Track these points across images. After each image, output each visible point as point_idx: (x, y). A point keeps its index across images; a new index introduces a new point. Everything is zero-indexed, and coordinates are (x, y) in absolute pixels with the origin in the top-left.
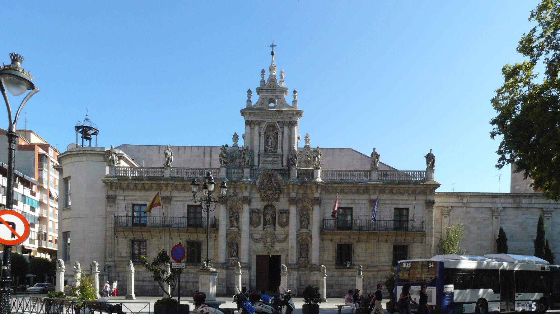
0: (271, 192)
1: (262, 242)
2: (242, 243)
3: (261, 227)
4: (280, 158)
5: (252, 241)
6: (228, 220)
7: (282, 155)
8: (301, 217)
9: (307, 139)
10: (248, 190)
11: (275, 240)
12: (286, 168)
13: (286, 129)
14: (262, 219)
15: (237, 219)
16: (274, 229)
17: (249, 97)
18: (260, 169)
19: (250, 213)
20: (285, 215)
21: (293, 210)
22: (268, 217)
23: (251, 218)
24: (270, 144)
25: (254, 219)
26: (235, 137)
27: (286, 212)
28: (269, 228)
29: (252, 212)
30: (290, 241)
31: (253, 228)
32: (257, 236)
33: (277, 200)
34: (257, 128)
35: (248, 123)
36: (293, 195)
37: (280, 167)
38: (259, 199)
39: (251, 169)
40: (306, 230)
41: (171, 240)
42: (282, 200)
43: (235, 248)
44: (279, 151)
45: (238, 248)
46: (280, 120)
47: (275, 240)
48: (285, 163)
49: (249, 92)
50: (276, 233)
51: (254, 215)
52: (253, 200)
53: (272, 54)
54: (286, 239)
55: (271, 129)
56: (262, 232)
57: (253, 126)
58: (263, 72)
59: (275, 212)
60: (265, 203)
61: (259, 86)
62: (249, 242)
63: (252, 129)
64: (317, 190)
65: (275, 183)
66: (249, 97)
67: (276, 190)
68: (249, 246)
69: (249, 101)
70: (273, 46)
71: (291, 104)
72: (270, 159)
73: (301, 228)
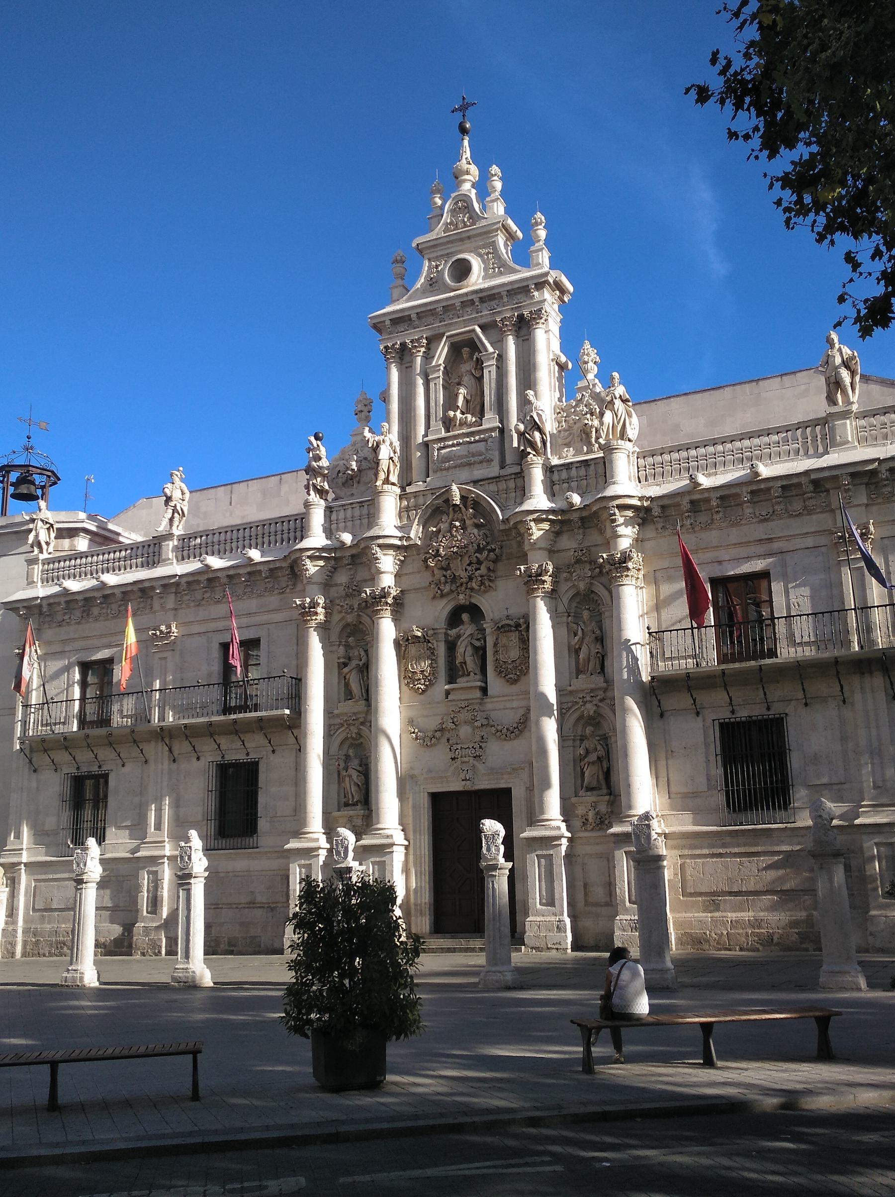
1: (444, 740)
12: (517, 469)
16: (484, 690)
20: (514, 637)
41: (174, 766)
43: (355, 775)
67: (479, 550)
73: (579, 672)
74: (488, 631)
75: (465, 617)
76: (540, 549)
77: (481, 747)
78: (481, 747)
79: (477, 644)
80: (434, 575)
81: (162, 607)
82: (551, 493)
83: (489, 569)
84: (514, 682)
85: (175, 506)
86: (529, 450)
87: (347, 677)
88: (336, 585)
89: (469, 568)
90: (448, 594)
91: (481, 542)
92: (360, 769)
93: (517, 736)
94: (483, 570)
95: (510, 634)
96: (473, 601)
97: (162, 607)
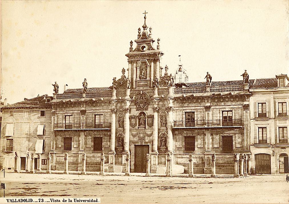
7: (150, 80)
13: (152, 64)
16: (145, 128)
17: (131, 46)
19: (129, 118)
21: (156, 115)
26: (124, 71)
27: (152, 117)
28: (142, 127)
29: (131, 118)
33: (146, 109)
34: (135, 64)
35: (130, 62)
38: (135, 110)
44: (148, 78)
49: (131, 43)
51: (133, 120)
53: (145, 18)
54: (152, 134)
57: (133, 63)
58: (139, 29)
63: (132, 65)
66: (131, 46)
69: (131, 49)
70: (145, 13)
71: (156, 48)
74: (146, 117)
79: (144, 119)
80: (137, 106)
81: (83, 107)
82: (159, 94)
85: (85, 87)
86: (155, 86)
94: (146, 107)
96: (144, 112)
97: (83, 107)
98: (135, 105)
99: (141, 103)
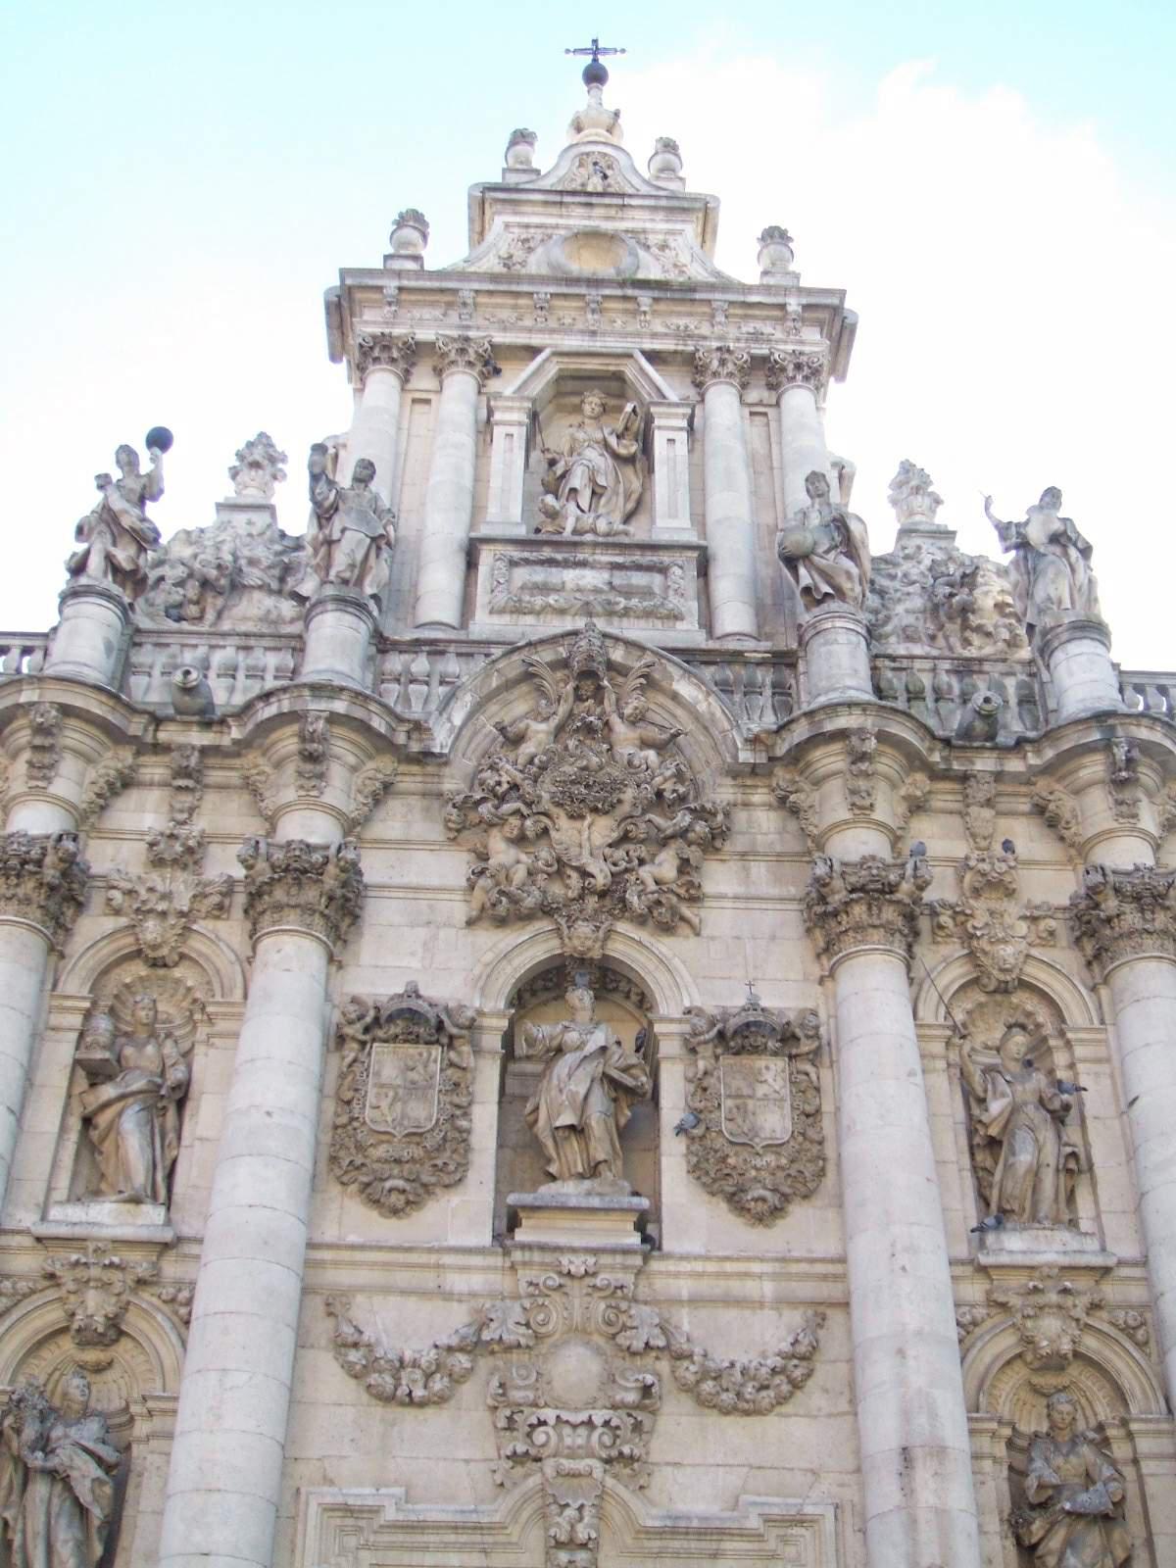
0: (602, 829)
2: (196, 1396)
3: (463, 1214)
4: (684, 576)
5: (330, 1380)
6: (47, 1114)
8: (974, 1099)
9: (911, 483)
10: (341, 787)
11: (661, 1374)
13: (723, 403)
14: (484, 1120)
15: (172, 1100)
18: (469, 649)
20: (773, 1072)
22: (569, 1090)
23: (343, 1100)
24: (577, 480)
25: (378, 1110)
27: (796, 1042)
30: (879, 1371)
31: (353, 1220)
32: (407, 1327)
36: (857, 844)
37: (688, 633)
38: (460, 911)
39: (382, 644)
40: (1063, 1236)
42: (717, 919)
45: (118, 1473)
46: (667, 345)
47: (661, 1374)
48: (734, 617)
50: (670, 1278)
51: (388, 1062)
52: (381, 914)
55: (592, 402)
56: (478, 1279)
57: (423, 380)
59: (646, 1045)
60: (530, 948)
61: (496, 178)
62: (295, 1399)
64: (1126, 811)
65: (645, 744)
68: (288, 1455)
72: (591, 578)
74: (669, 1047)
75: (581, 997)
76: (881, 826)
77: (637, 1427)
78: (637, 1427)
83: (684, 867)
84: (769, 1214)
87: (103, 1120)
88: (118, 835)
89: (620, 853)
90: (528, 917)
91: (668, 786)
92: (108, 1453)
93: (781, 1400)
94: (666, 865)
95: (761, 1062)
96: (618, 949)
98: (456, 833)
99: (589, 797)
